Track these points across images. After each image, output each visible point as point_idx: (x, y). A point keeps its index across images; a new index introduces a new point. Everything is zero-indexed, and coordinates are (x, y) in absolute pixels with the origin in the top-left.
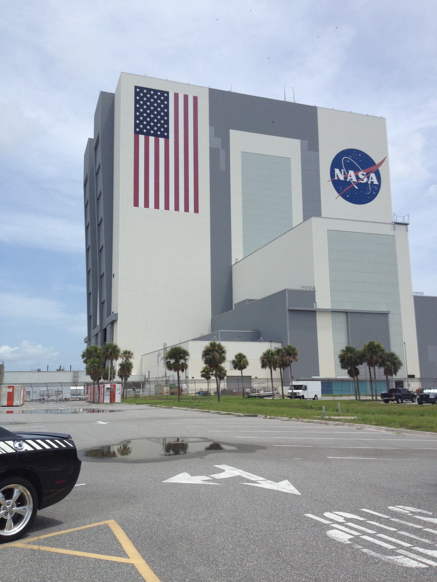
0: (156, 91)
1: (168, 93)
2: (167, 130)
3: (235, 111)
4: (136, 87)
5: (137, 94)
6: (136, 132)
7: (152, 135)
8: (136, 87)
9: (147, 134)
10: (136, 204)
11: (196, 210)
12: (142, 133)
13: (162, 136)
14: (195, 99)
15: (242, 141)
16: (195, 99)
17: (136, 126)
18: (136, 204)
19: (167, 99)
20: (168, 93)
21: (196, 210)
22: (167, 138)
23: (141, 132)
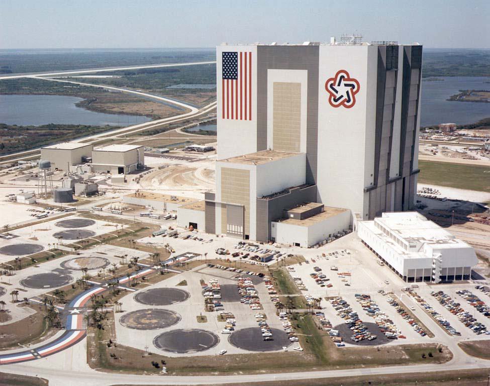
0: (231, 53)
1: (237, 53)
2: (237, 75)
3: (274, 56)
4: (223, 53)
5: (223, 56)
6: (223, 78)
7: (230, 79)
8: (223, 53)
9: (228, 79)
10: (224, 117)
11: (250, 119)
12: (226, 78)
13: (235, 78)
14: (250, 53)
15: (275, 76)
16: (250, 53)
17: (223, 74)
18: (224, 117)
19: (237, 56)
20: (237, 53)
21: (250, 119)
22: (237, 79)
23: (225, 78)
